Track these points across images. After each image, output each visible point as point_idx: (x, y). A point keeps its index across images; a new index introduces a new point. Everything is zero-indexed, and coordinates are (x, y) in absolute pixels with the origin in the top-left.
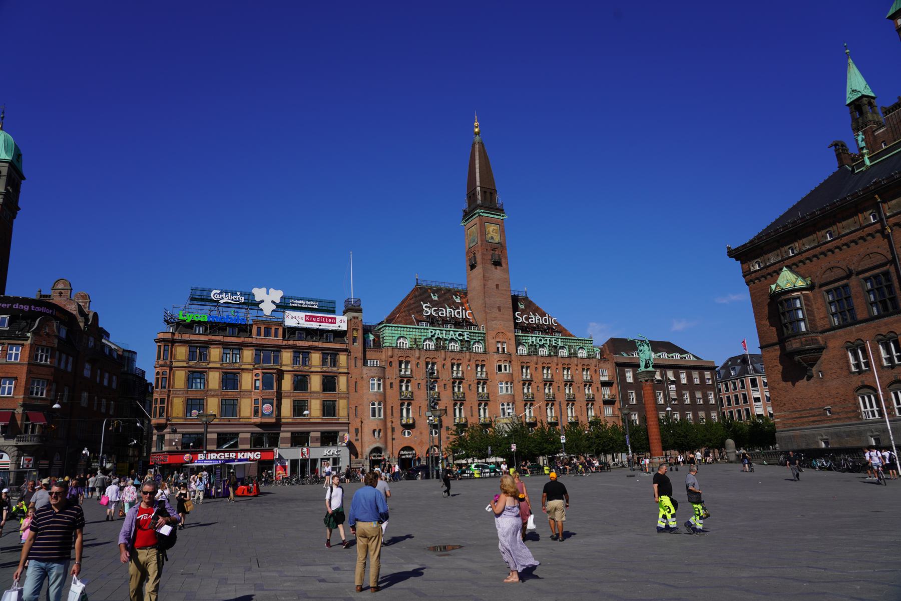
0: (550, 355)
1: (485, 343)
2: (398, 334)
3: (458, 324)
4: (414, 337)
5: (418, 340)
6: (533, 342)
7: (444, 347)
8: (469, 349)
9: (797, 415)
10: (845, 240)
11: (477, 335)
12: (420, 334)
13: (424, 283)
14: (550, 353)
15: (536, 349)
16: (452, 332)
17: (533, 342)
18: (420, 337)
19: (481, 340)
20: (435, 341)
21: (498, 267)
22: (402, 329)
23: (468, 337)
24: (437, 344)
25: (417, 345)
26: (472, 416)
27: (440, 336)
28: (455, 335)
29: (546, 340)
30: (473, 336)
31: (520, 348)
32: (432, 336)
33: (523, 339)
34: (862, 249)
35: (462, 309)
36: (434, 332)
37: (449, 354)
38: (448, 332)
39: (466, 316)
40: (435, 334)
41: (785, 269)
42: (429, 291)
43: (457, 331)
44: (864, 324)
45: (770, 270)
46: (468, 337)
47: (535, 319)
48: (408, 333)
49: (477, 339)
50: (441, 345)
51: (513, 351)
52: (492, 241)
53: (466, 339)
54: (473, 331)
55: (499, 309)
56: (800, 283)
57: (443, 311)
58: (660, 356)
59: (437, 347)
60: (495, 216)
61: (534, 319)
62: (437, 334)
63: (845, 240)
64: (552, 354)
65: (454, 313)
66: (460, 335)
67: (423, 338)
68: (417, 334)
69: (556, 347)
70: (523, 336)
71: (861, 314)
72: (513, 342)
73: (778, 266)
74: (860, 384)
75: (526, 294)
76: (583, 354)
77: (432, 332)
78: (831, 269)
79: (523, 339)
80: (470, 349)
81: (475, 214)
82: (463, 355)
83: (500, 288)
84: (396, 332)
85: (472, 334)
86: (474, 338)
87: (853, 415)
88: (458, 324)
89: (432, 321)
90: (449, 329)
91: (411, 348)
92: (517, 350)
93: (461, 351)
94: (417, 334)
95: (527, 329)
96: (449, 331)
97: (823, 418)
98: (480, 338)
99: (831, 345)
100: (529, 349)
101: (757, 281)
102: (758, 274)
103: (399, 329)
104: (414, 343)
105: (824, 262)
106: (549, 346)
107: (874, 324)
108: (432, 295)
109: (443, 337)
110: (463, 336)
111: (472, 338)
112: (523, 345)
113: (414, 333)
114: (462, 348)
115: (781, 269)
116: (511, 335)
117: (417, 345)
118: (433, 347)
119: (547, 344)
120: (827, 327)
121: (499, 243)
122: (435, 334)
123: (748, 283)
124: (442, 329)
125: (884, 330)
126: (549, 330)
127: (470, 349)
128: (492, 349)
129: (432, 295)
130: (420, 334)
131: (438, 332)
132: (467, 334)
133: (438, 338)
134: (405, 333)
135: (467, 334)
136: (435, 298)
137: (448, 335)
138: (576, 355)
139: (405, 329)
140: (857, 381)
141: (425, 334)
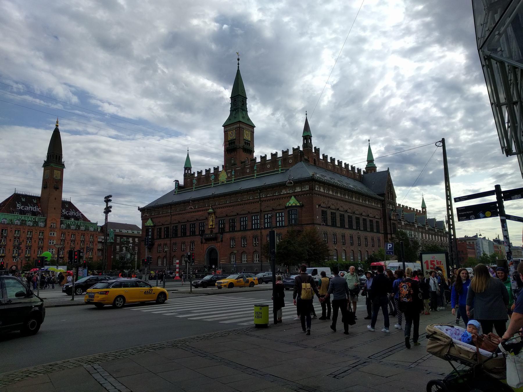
0: (76, 229)
1: (45, 223)
2: (3, 217)
3: (34, 214)
4: (11, 219)
5: (12, 220)
6: (69, 223)
7: (25, 224)
8: (37, 225)
11: (42, 219)
12: (14, 218)
13: (19, 193)
14: (76, 228)
15: (70, 226)
16: (30, 218)
17: (69, 223)
18: (14, 219)
19: (44, 222)
20: (21, 221)
21: (57, 190)
22: (5, 215)
23: (37, 220)
24: (22, 222)
25: (12, 223)
26: (34, 253)
27: (24, 219)
28: (31, 219)
29: (75, 223)
30: (40, 220)
31: (63, 225)
32: (20, 219)
33: (64, 222)
35: (37, 207)
36: (21, 217)
37: (27, 227)
38: (28, 217)
39: (38, 210)
40: (21, 218)
41: (150, 219)
42: (21, 196)
43: (32, 217)
46: (37, 220)
47: (72, 213)
48: (8, 217)
49: (42, 221)
50: (23, 223)
51: (58, 226)
52: (56, 178)
53: (36, 221)
54: (40, 217)
55: (55, 209)
56: (152, 225)
57: (27, 207)
58: (128, 232)
59: (22, 224)
60: (60, 167)
61: (71, 213)
62: (22, 218)
64: (77, 228)
65: (32, 208)
66: (33, 219)
67: (15, 219)
68: (12, 217)
69: (80, 226)
70: (64, 221)
71: (163, 237)
72: (59, 223)
75: (70, 200)
76: (92, 229)
77: (20, 217)
79: (64, 222)
80: (38, 225)
81: (50, 165)
82: (34, 227)
83: (57, 199)
84: (2, 216)
85: (40, 219)
86: (41, 220)
88: (34, 214)
89: (22, 212)
90: (29, 216)
91: (8, 224)
92: (60, 226)
93: (33, 226)
94: (12, 217)
95: (68, 217)
96: (29, 217)
98: (43, 221)
100: (66, 226)
103: (4, 215)
104: (10, 221)
106: (76, 226)
108: (22, 198)
109: (25, 220)
110: (36, 219)
111: (39, 220)
112: (64, 224)
113: (11, 217)
114: (34, 225)
116: (59, 220)
117: (12, 223)
118: (20, 224)
119: (75, 224)
121: (59, 180)
122: (21, 218)
123: (142, 220)
124: (25, 216)
126: (77, 218)
127: (38, 225)
128: (48, 225)
129: (22, 198)
130: (14, 218)
131: (23, 217)
132: (37, 219)
133: (23, 220)
134: (6, 217)
135: (37, 219)
136: (23, 200)
137: (28, 219)
138: (88, 229)
139: (7, 215)
141: (16, 218)
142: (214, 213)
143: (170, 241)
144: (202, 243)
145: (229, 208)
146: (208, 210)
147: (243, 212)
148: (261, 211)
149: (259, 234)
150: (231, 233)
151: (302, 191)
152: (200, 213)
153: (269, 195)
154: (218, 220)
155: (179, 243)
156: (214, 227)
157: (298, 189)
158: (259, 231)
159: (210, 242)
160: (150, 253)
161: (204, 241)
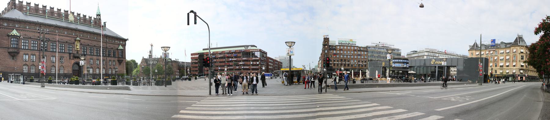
9: (6, 68)
10: (31, 30)
34: (33, 34)
44: (29, 50)
45: (9, 27)
63: (31, 30)
73: (12, 28)
74: (25, 64)
78: (25, 35)
87: (21, 70)
97: (13, 70)
99: (21, 53)
101: (4, 29)
102: (5, 27)
105: (24, 33)
107: (31, 51)
115: (13, 29)
120: (21, 48)
125: (33, 53)
140: (24, 63)
142: (75, 40)
143: (40, 53)
144: (70, 59)
145: (89, 41)
146: (76, 38)
147: (92, 45)
148: (107, 47)
149: (106, 59)
150: (91, 56)
151: (122, 44)
152: (69, 38)
153: (110, 41)
154: (82, 46)
155: (49, 56)
156: (79, 50)
157: (121, 42)
158: (106, 58)
159: (76, 59)
160: (13, 60)
161: (71, 58)
